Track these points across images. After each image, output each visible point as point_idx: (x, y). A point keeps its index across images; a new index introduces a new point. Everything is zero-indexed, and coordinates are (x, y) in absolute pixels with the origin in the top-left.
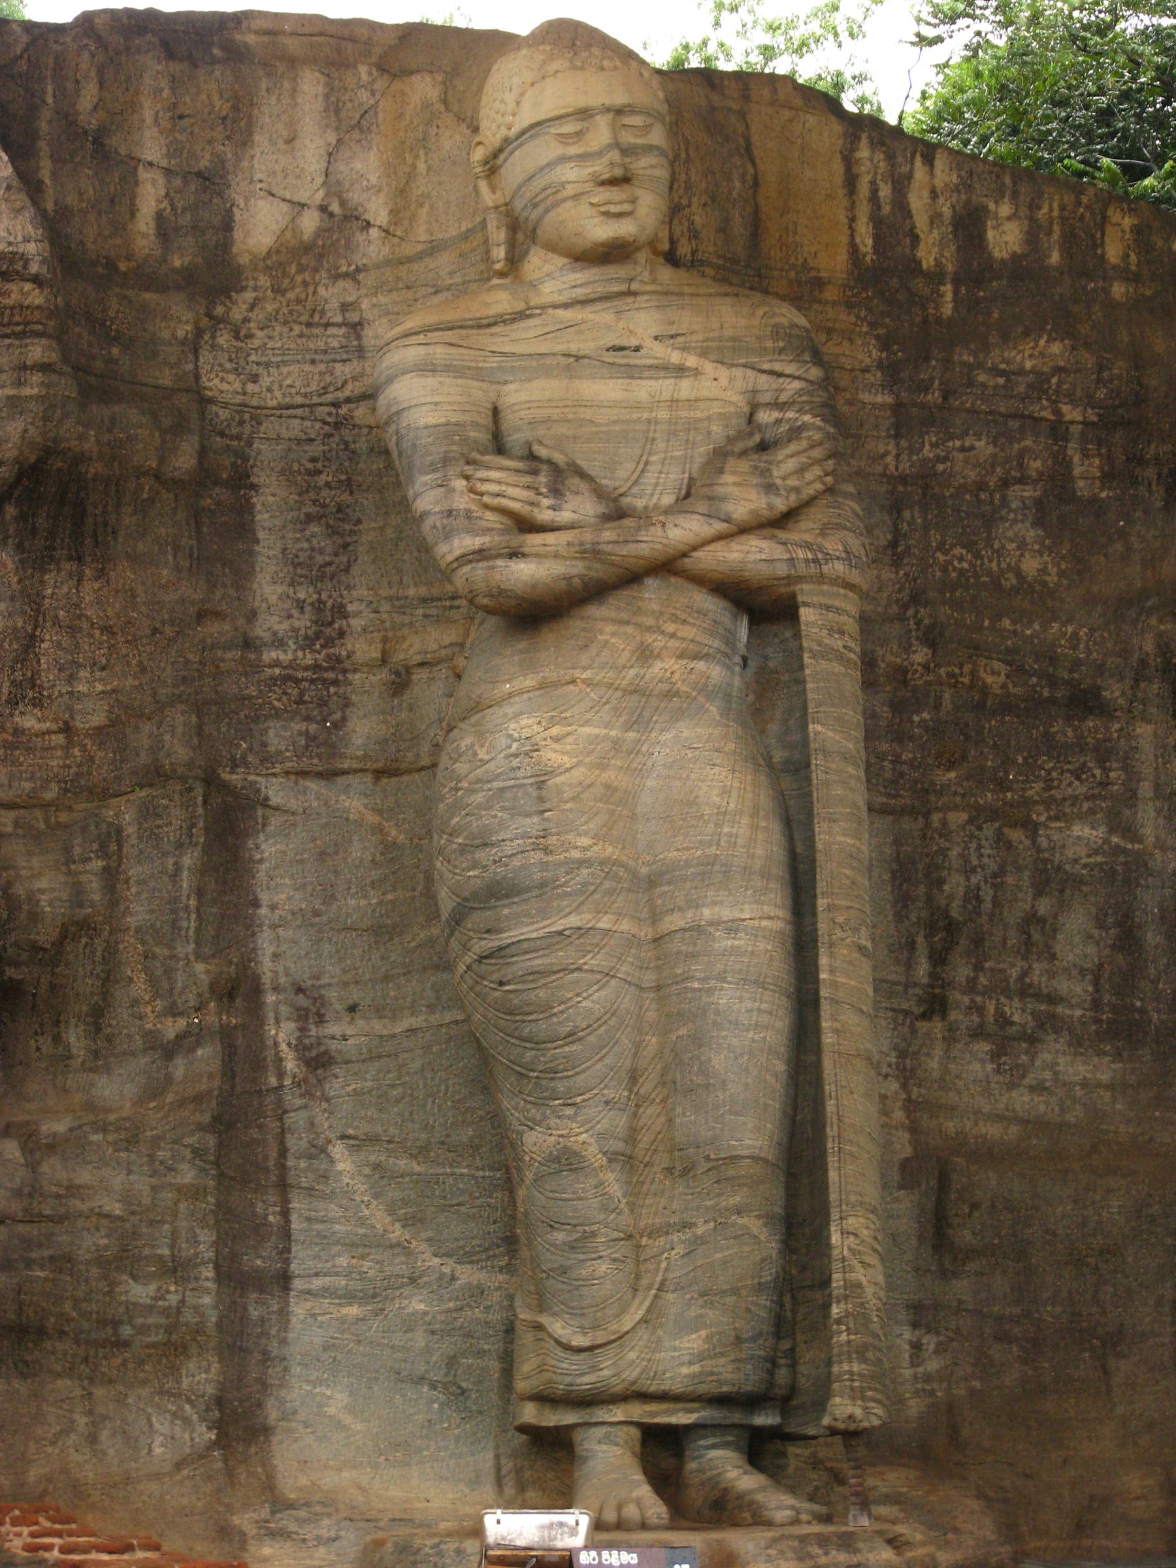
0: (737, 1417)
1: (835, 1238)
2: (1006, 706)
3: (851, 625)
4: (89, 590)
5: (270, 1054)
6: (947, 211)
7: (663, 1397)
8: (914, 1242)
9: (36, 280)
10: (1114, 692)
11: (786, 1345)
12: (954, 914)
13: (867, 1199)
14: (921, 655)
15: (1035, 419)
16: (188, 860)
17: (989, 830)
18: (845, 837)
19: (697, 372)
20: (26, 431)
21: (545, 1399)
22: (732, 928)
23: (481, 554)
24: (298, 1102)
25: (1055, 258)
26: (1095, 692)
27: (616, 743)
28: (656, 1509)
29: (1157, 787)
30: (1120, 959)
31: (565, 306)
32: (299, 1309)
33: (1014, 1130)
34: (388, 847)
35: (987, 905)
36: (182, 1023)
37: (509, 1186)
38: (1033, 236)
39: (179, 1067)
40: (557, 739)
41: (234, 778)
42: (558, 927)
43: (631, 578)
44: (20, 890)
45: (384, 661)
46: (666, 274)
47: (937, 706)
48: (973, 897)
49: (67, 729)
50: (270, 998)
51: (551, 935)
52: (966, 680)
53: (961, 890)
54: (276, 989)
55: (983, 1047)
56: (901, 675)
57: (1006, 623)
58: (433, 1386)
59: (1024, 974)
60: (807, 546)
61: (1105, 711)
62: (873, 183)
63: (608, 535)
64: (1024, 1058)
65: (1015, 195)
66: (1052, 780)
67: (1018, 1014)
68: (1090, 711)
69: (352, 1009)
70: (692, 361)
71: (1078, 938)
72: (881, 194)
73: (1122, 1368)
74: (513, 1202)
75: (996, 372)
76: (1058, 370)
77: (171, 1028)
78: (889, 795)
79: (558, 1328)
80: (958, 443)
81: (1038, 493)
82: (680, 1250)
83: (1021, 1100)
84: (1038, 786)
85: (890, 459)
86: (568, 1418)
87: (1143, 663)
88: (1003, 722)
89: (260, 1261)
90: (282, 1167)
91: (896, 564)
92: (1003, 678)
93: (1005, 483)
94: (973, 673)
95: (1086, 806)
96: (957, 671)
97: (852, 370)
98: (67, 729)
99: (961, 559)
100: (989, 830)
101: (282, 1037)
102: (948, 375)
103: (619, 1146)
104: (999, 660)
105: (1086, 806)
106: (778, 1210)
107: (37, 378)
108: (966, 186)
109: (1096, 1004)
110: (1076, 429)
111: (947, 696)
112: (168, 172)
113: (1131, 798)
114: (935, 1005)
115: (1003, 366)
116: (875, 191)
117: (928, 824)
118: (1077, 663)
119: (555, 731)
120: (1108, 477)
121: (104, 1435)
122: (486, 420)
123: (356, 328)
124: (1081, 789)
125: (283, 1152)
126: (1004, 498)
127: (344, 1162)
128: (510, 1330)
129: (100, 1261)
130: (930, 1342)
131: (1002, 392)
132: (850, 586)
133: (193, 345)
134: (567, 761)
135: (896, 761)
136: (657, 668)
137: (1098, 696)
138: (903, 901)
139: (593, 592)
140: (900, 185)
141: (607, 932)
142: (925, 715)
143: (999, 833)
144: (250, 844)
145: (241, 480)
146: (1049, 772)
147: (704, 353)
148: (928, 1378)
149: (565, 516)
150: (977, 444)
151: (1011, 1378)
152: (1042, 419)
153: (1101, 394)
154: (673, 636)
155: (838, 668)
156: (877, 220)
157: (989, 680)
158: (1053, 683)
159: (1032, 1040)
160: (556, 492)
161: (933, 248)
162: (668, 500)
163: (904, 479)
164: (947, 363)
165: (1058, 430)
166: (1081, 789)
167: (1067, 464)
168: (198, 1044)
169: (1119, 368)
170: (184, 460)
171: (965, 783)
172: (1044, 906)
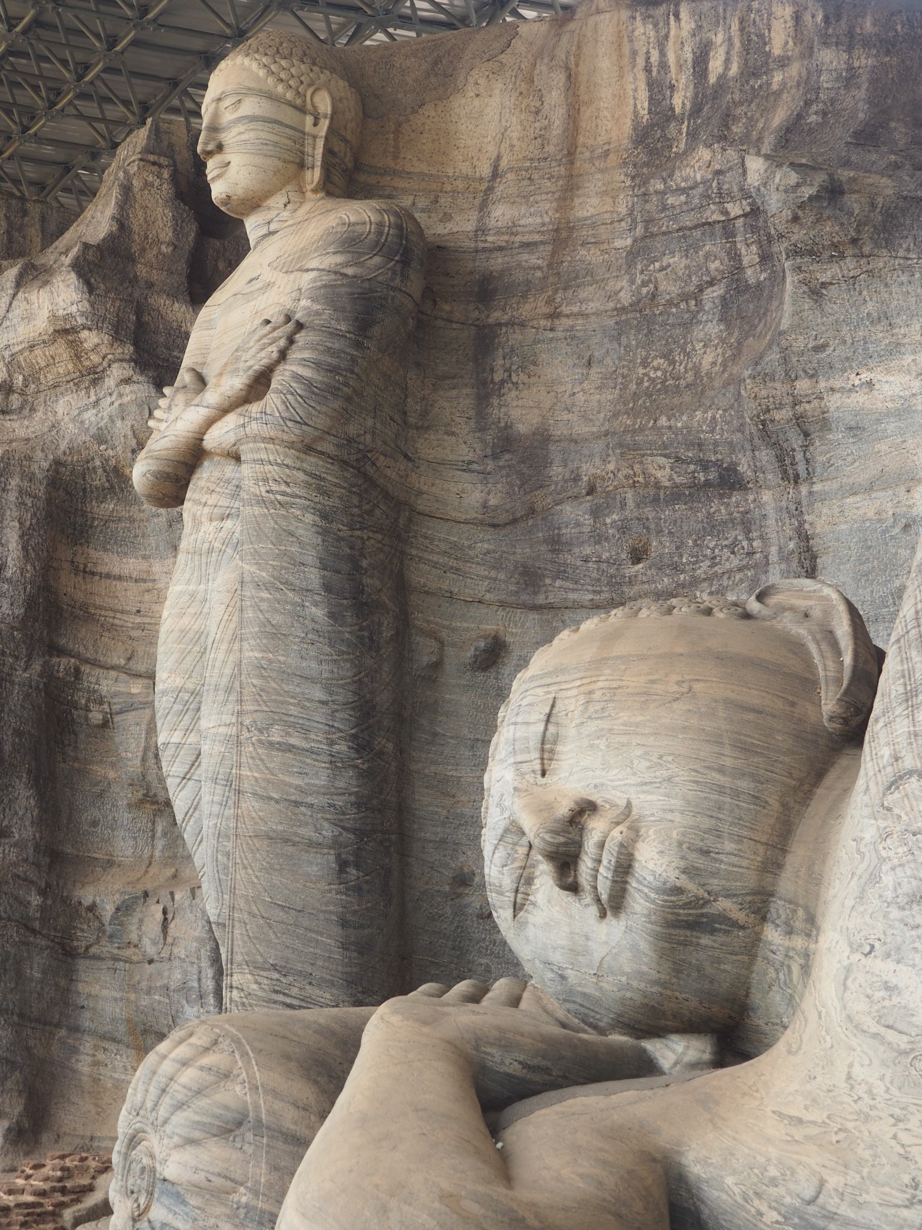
2: (676, 495)
6: (689, 56)
10: (744, 468)
15: (709, 224)
20: (132, 426)
26: (732, 469)
27: (193, 595)
47: (623, 505)
52: (641, 479)
57: (663, 421)
66: (714, 558)
68: (732, 488)
72: (652, 60)
76: (718, 173)
78: (594, 591)
80: (657, 265)
81: (722, 291)
88: (674, 511)
95: (738, 576)
96: (631, 472)
97: (611, 223)
102: (648, 207)
104: (661, 455)
105: (738, 576)
107: (128, 389)
110: (740, 222)
111: (630, 495)
115: (683, 184)
118: (716, 444)
131: (685, 208)
132: (272, 440)
141: (179, 745)
142: (615, 517)
146: (713, 550)
150: (671, 261)
152: (714, 222)
155: (257, 510)
156: (650, 85)
157: (659, 474)
158: (705, 466)
166: (735, 562)
167: (735, 256)
171: (649, 573)
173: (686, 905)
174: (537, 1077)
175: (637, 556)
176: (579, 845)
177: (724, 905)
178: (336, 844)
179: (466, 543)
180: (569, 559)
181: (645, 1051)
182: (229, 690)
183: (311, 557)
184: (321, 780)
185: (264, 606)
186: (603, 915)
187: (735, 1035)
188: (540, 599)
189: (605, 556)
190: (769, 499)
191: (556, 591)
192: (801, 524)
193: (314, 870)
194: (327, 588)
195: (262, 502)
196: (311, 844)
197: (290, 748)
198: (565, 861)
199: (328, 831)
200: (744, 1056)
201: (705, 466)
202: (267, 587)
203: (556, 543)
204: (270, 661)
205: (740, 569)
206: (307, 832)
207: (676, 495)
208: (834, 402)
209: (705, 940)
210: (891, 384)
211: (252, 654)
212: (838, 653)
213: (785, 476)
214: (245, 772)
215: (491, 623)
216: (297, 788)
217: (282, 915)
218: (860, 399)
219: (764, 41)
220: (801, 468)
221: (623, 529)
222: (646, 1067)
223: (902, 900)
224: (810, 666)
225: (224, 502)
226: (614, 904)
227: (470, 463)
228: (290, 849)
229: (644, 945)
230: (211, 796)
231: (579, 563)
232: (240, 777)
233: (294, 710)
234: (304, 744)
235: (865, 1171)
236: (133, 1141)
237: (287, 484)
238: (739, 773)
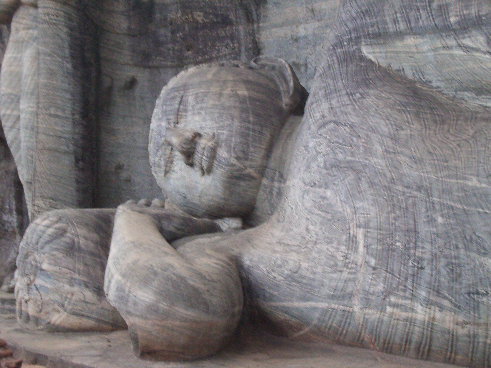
2: (205, 26)
10: (232, 17)
13: (45, 195)
27: (15, 58)
47: (184, 29)
52: (191, 20)
61: (231, 23)
78: (172, 62)
84: (215, 52)
92: (202, 18)
94: (193, 18)
118: (221, 8)
124: (227, 51)
135: (174, 50)
141: (9, 115)
155: (45, 26)
157: (198, 18)
158: (217, 16)
166: (227, 51)
173: (237, 171)
174: (180, 232)
176: (195, 149)
177: (250, 171)
178: (75, 153)
179: (121, 42)
180: (162, 49)
181: (215, 224)
182: (32, 94)
183: (66, 45)
184: (69, 128)
185: (48, 62)
186: (203, 174)
187: (248, 217)
188: (151, 64)
189: (176, 48)
191: (157, 60)
192: (254, 37)
193: (67, 162)
194: (72, 56)
195: (47, 22)
196: (66, 153)
197: (58, 116)
198: (189, 155)
199: (72, 148)
200: (251, 226)
202: (50, 55)
203: (158, 43)
204: (50, 83)
205: (229, 54)
206: (64, 148)
209: (242, 183)
211: (42, 80)
212: (287, 82)
214: (40, 125)
215: (130, 72)
216: (61, 132)
217: (54, 178)
220: (255, 17)
221: (184, 39)
222: (213, 229)
223: (328, 166)
224: (277, 86)
225: (29, 23)
226: (207, 171)
227: (123, 12)
228: (57, 154)
229: (219, 185)
230: (23, 135)
231: (166, 51)
232: (38, 127)
233: (59, 102)
234: (63, 115)
235: (316, 261)
236: (27, 256)
237: (57, 16)
238: (255, 124)
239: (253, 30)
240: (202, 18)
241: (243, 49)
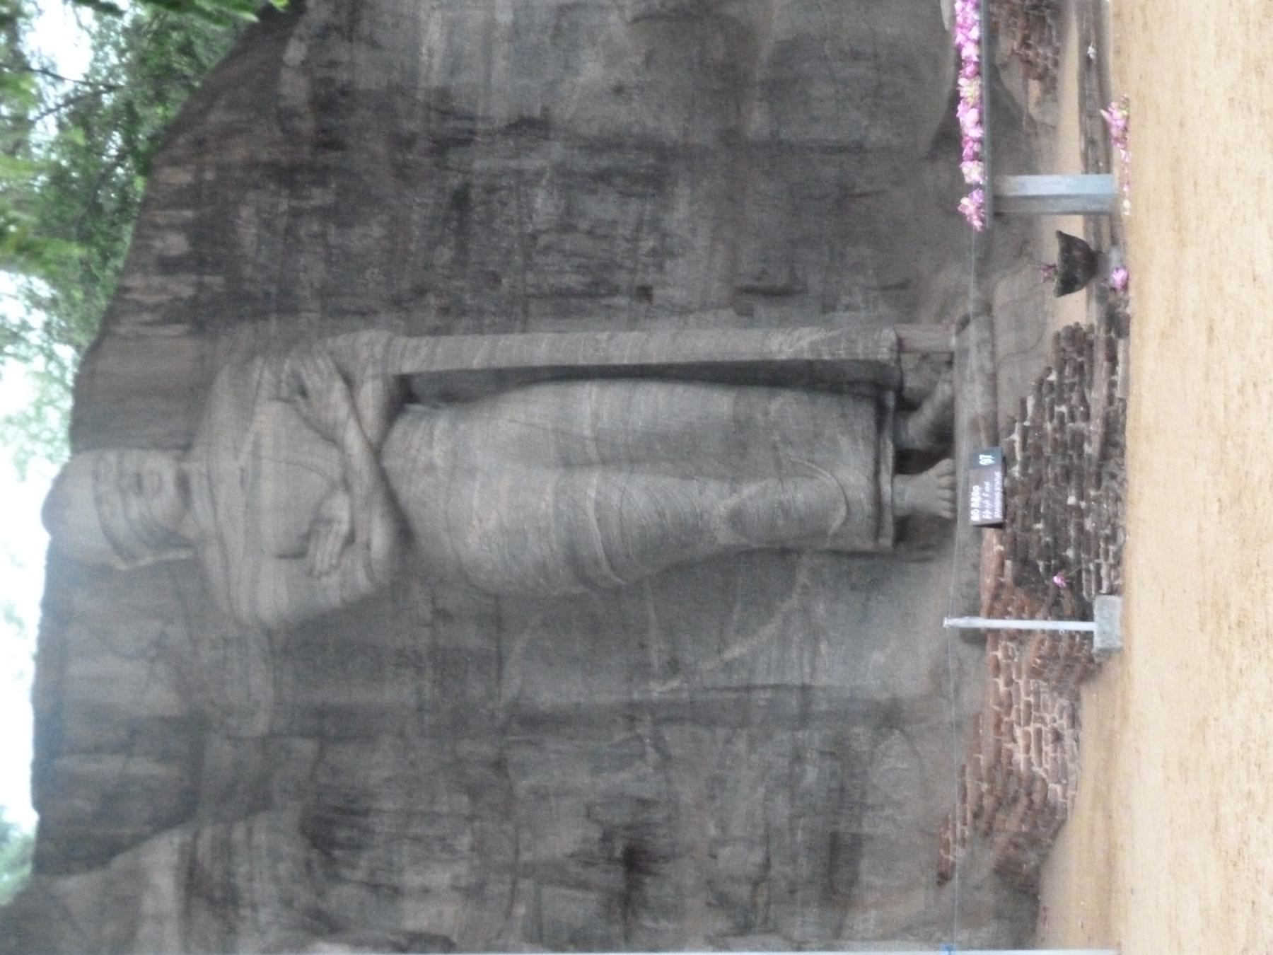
0: (889, 419)
1: (783, 357)
2: (462, 248)
3: (414, 342)
4: (388, 805)
5: (670, 697)
7: (877, 462)
8: (785, 308)
9: (196, 836)
10: (455, 181)
11: (846, 387)
12: (588, 279)
14: (431, 300)
16: (550, 744)
17: (539, 259)
18: (541, 345)
19: (258, 435)
21: (877, 533)
22: (596, 416)
23: (368, 565)
24: (698, 679)
25: (189, 214)
27: (483, 485)
28: (944, 465)
29: (511, 157)
30: (619, 180)
31: (215, 514)
32: (822, 680)
33: (720, 247)
34: (544, 624)
35: (583, 260)
36: (650, 750)
37: (750, 553)
38: (172, 227)
39: (676, 752)
40: (480, 520)
41: (501, 716)
42: (595, 523)
43: (383, 477)
44: (569, 851)
45: (431, 625)
46: (198, 451)
47: (462, 289)
48: (579, 269)
49: (470, 818)
50: (636, 696)
51: (599, 526)
53: (574, 277)
54: (630, 693)
55: (669, 264)
56: (445, 311)
57: (413, 247)
58: (868, 599)
59: (627, 240)
60: (364, 368)
61: (467, 186)
62: (142, 324)
63: (357, 490)
64: (676, 240)
65: (150, 237)
67: (649, 243)
69: (642, 646)
70: (251, 438)
71: (601, 206)
73: (862, 186)
74: (761, 550)
75: (258, 251)
77: (652, 756)
79: (836, 522)
82: (790, 451)
83: (701, 242)
85: (311, 315)
86: (888, 519)
87: (437, 165)
89: (793, 703)
90: (736, 690)
91: (376, 313)
93: (327, 247)
98: (470, 818)
99: (374, 274)
100: (539, 259)
101: (659, 689)
103: (727, 486)
106: (763, 391)
108: (144, 268)
109: (642, 196)
110: (295, 203)
112: (130, 755)
113: (519, 173)
114: (645, 293)
116: (148, 324)
117: (533, 296)
119: (475, 522)
120: (323, 183)
121: (895, 797)
122: (284, 563)
123: (227, 641)
124: (514, 203)
125: (729, 689)
126: (337, 247)
127: (735, 651)
128: (836, 553)
129: (792, 798)
130: (845, 299)
133: (236, 740)
134: (494, 515)
136: (439, 462)
137: (457, 192)
138: (581, 312)
139: (392, 499)
140: (142, 307)
141: (599, 493)
142: (467, 296)
143: (539, 253)
144: (542, 708)
145: (321, 712)
147: (246, 429)
148: (867, 302)
149: (344, 515)
151: (866, 251)
153: (272, 186)
154: (418, 450)
158: (447, 220)
159: (665, 235)
160: (329, 522)
161: (183, 287)
162: (335, 452)
163: (323, 308)
164: (251, 281)
165: (296, 214)
166: (514, 203)
167: (315, 210)
168: (661, 738)
169: (256, 175)
170: (306, 748)
172: (584, 225)
175: (495, 279)
190: (481, 163)
201: (447, 220)
207: (462, 248)
208: (435, 81)
210: (434, 35)
213: (467, 142)
218: (437, 61)
219: (180, 191)
220: (467, 125)
239: (488, 133)
240: (446, 250)
241: (513, 164)
